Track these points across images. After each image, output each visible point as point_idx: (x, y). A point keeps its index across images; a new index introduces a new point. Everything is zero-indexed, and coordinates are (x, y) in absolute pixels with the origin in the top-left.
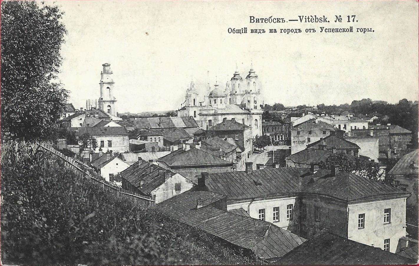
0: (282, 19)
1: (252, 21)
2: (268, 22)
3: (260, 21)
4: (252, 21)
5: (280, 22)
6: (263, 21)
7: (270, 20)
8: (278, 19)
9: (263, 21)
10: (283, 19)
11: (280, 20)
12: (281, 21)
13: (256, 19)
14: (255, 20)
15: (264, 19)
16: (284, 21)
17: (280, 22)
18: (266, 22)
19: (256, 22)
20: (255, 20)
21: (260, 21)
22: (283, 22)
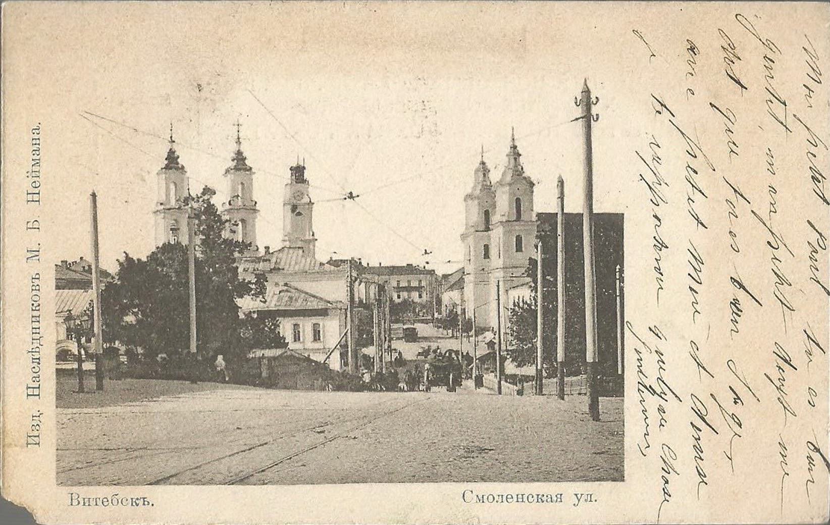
0: (142, 500)
1: (75, 502)
2: (110, 504)
3: (93, 503)
4: (75, 502)
5: (137, 505)
6: (99, 503)
7: (115, 502)
8: (134, 500)
9: (99, 503)
10: (144, 498)
11: (137, 501)
12: (141, 502)
13: (84, 499)
14: (81, 500)
15: (101, 499)
16: (146, 503)
17: (137, 505)
18: (106, 504)
19: (84, 505)
20: (81, 500)
21: (93, 503)
22: (144, 504)
